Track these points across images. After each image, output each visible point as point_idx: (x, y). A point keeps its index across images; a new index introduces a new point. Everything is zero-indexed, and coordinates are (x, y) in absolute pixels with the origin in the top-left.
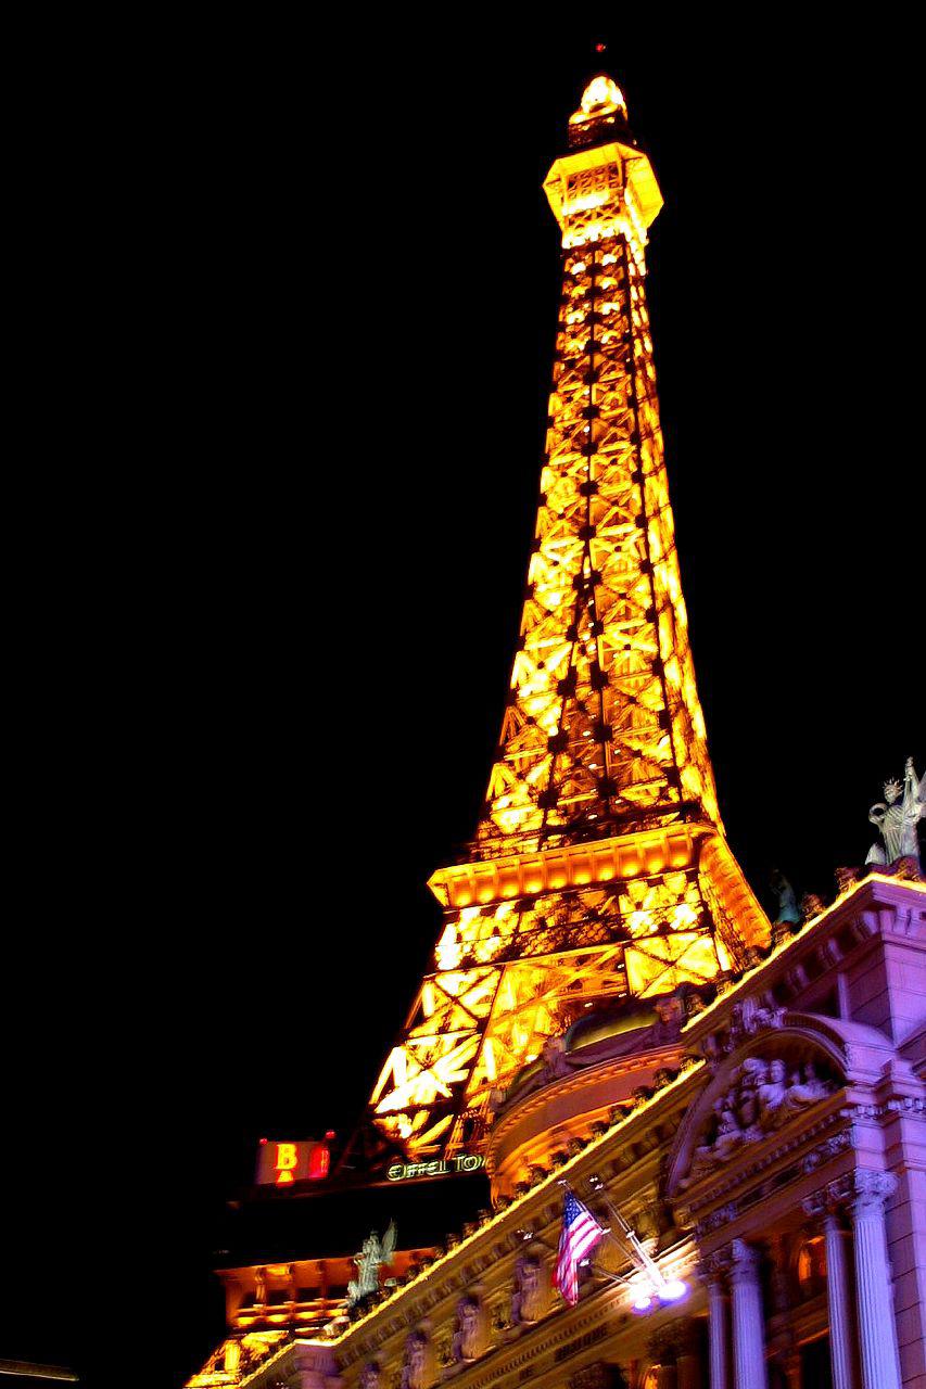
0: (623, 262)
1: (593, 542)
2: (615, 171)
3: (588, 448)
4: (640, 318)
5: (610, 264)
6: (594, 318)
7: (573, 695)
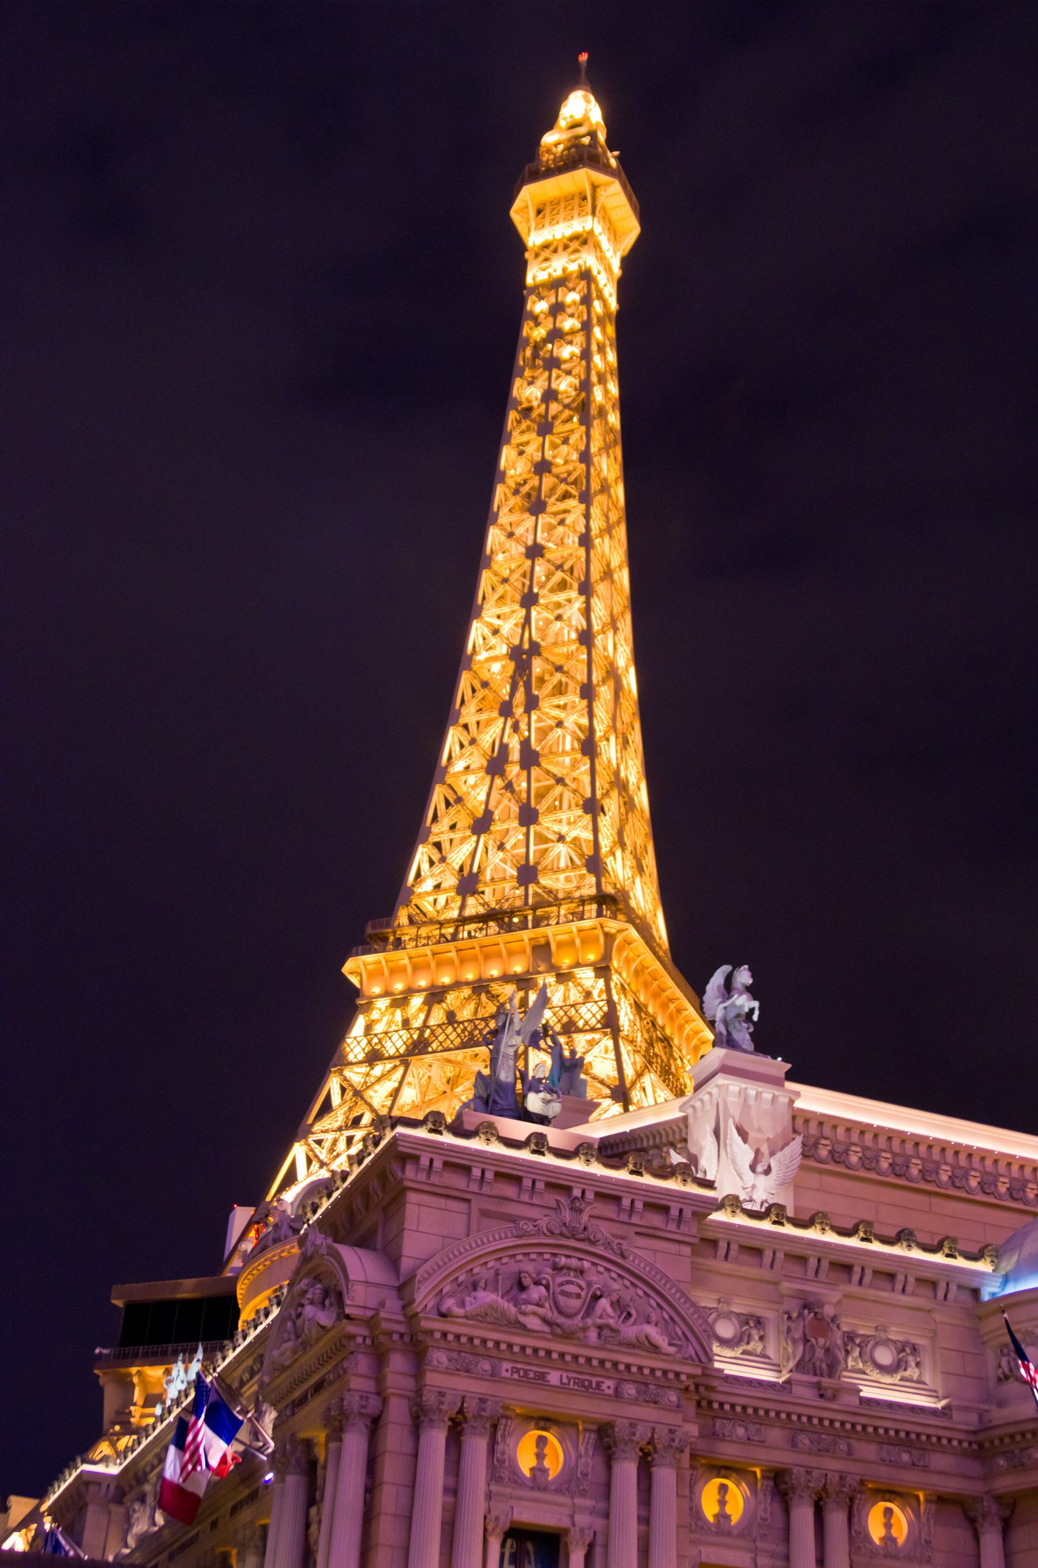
0: (587, 300)
2: (585, 198)
3: (536, 506)
5: (574, 303)
7: (502, 774)
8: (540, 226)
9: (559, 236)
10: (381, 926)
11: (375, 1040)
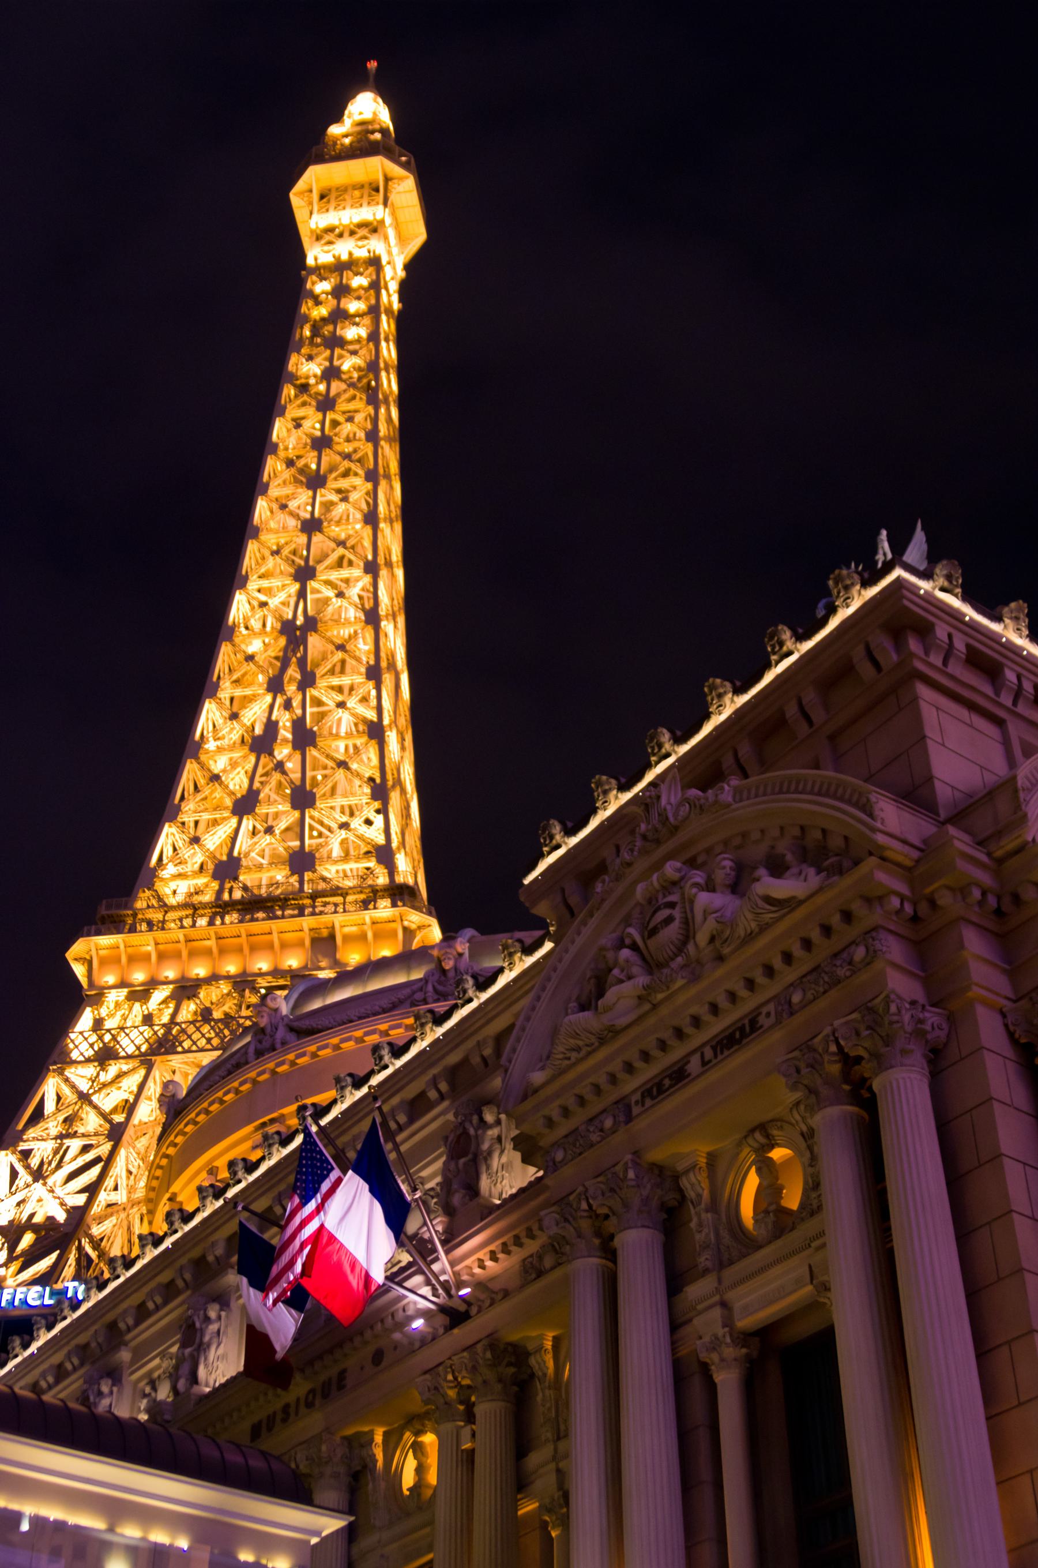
1: (312, 584)
2: (377, 190)
3: (315, 482)
4: (389, 352)
5: (361, 287)
9: (346, 221)
10: (119, 907)
11: (107, 1038)
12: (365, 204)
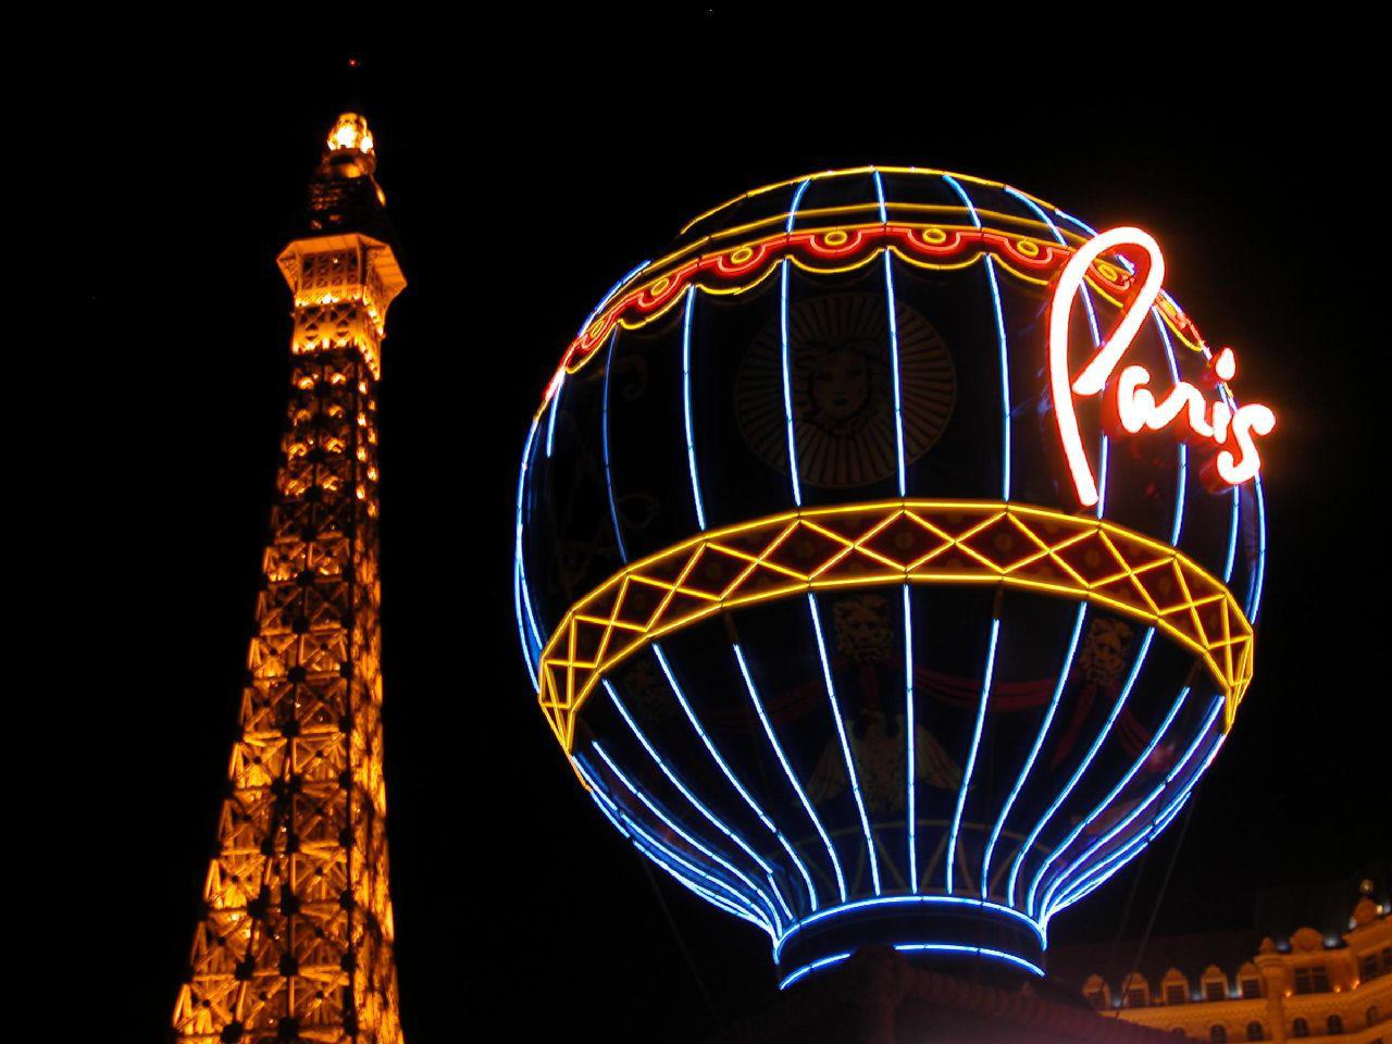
2: (354, 261)
3: (297, 622)
6: (317, 456)
8: (307, 285)
12: (345, 282)
